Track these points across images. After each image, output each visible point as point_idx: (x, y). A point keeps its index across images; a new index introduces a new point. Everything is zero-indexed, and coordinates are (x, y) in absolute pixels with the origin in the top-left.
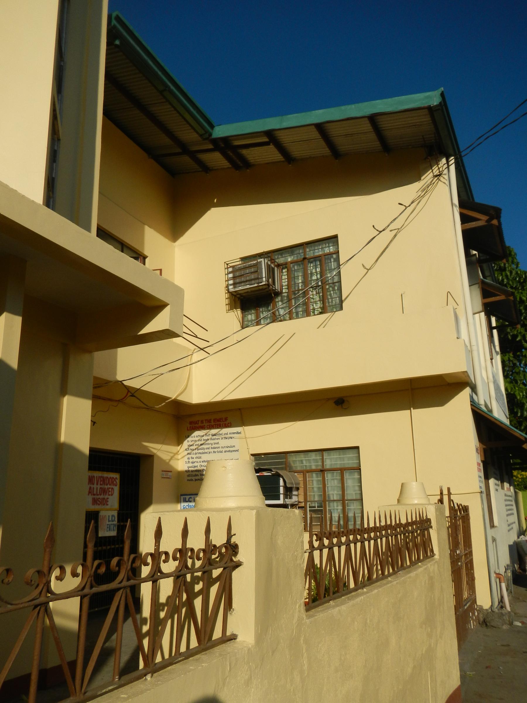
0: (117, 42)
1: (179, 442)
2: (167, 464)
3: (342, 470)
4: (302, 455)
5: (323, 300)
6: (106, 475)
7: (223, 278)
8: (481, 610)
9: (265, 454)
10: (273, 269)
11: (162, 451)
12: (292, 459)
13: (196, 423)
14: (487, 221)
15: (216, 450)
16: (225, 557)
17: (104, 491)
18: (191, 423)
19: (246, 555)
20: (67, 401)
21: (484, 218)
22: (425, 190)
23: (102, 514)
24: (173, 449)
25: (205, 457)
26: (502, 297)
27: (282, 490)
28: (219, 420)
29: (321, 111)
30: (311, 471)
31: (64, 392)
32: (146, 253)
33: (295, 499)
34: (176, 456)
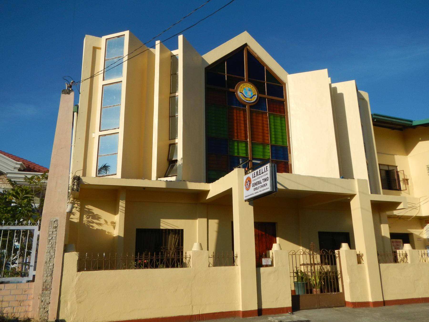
0: (375, 120)
1: (423, 227)
2: (419, 236)
11: (416, 232)
13: (428, 221)
16: (406, 255)
17: (398, 245)
18: (426, 221)
19: (408, 254)
20: (382, 226)
24: (421, 230)
31: (381, 223)
32: (397, 165)
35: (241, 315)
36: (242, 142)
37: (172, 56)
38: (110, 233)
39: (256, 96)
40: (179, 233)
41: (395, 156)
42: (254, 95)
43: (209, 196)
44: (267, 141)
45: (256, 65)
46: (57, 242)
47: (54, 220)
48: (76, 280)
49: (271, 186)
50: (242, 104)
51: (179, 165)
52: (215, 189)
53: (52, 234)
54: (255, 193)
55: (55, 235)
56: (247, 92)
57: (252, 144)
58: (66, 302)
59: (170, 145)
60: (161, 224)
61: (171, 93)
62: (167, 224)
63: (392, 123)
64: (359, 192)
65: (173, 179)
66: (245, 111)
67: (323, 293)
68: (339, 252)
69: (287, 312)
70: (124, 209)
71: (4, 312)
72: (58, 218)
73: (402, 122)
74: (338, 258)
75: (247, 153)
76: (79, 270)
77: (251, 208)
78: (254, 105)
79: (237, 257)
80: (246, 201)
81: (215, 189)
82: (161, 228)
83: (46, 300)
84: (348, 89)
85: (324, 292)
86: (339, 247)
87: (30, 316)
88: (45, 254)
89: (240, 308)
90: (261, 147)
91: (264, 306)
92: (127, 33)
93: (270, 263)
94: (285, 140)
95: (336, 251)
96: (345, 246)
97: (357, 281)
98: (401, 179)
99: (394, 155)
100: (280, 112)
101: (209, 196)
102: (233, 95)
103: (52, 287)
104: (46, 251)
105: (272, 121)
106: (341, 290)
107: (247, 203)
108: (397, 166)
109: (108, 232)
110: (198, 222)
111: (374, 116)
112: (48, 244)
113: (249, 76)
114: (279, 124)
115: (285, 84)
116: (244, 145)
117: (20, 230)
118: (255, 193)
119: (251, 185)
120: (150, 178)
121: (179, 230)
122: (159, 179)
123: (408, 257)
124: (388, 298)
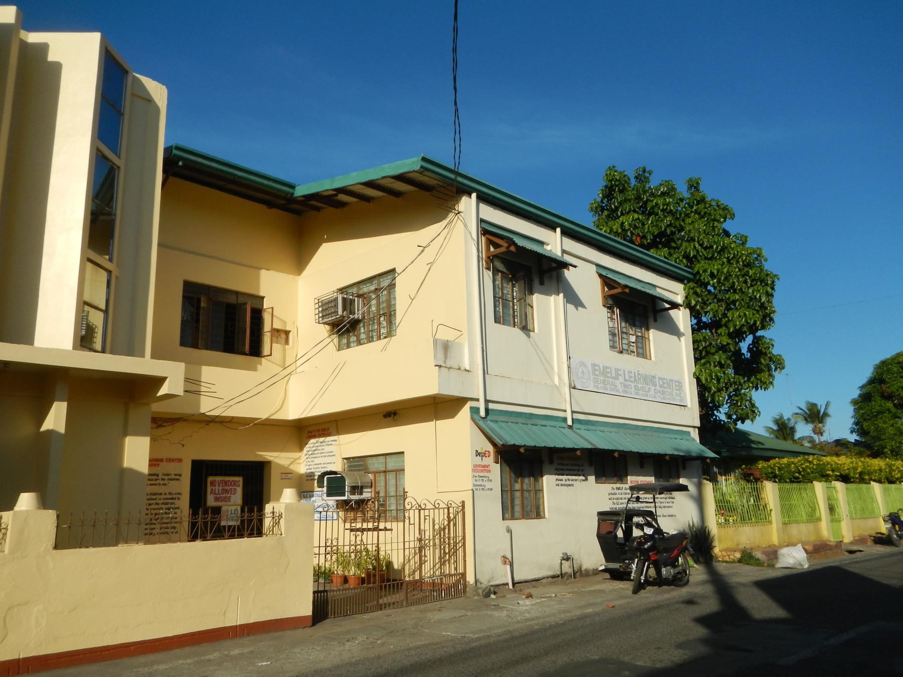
1: (301, 449)
4: (375, 458)
6: (227, 478)
9: (353, 458)
10: (352, 301)
11: (279, 458)
14: (508, 247)
17: (227, 491)
18: (309, 432)
23: (224, 509)
25: (317, 461)
26: (619, 290)
28: (324, 430)
29: (354, 174)
31: (126, 433)
32: (262, 294)
34: (298, 461)
41: (263, 272)
98: (267, 327)
99: (261, 269)
108: (263, 298)
111: (174, 152)
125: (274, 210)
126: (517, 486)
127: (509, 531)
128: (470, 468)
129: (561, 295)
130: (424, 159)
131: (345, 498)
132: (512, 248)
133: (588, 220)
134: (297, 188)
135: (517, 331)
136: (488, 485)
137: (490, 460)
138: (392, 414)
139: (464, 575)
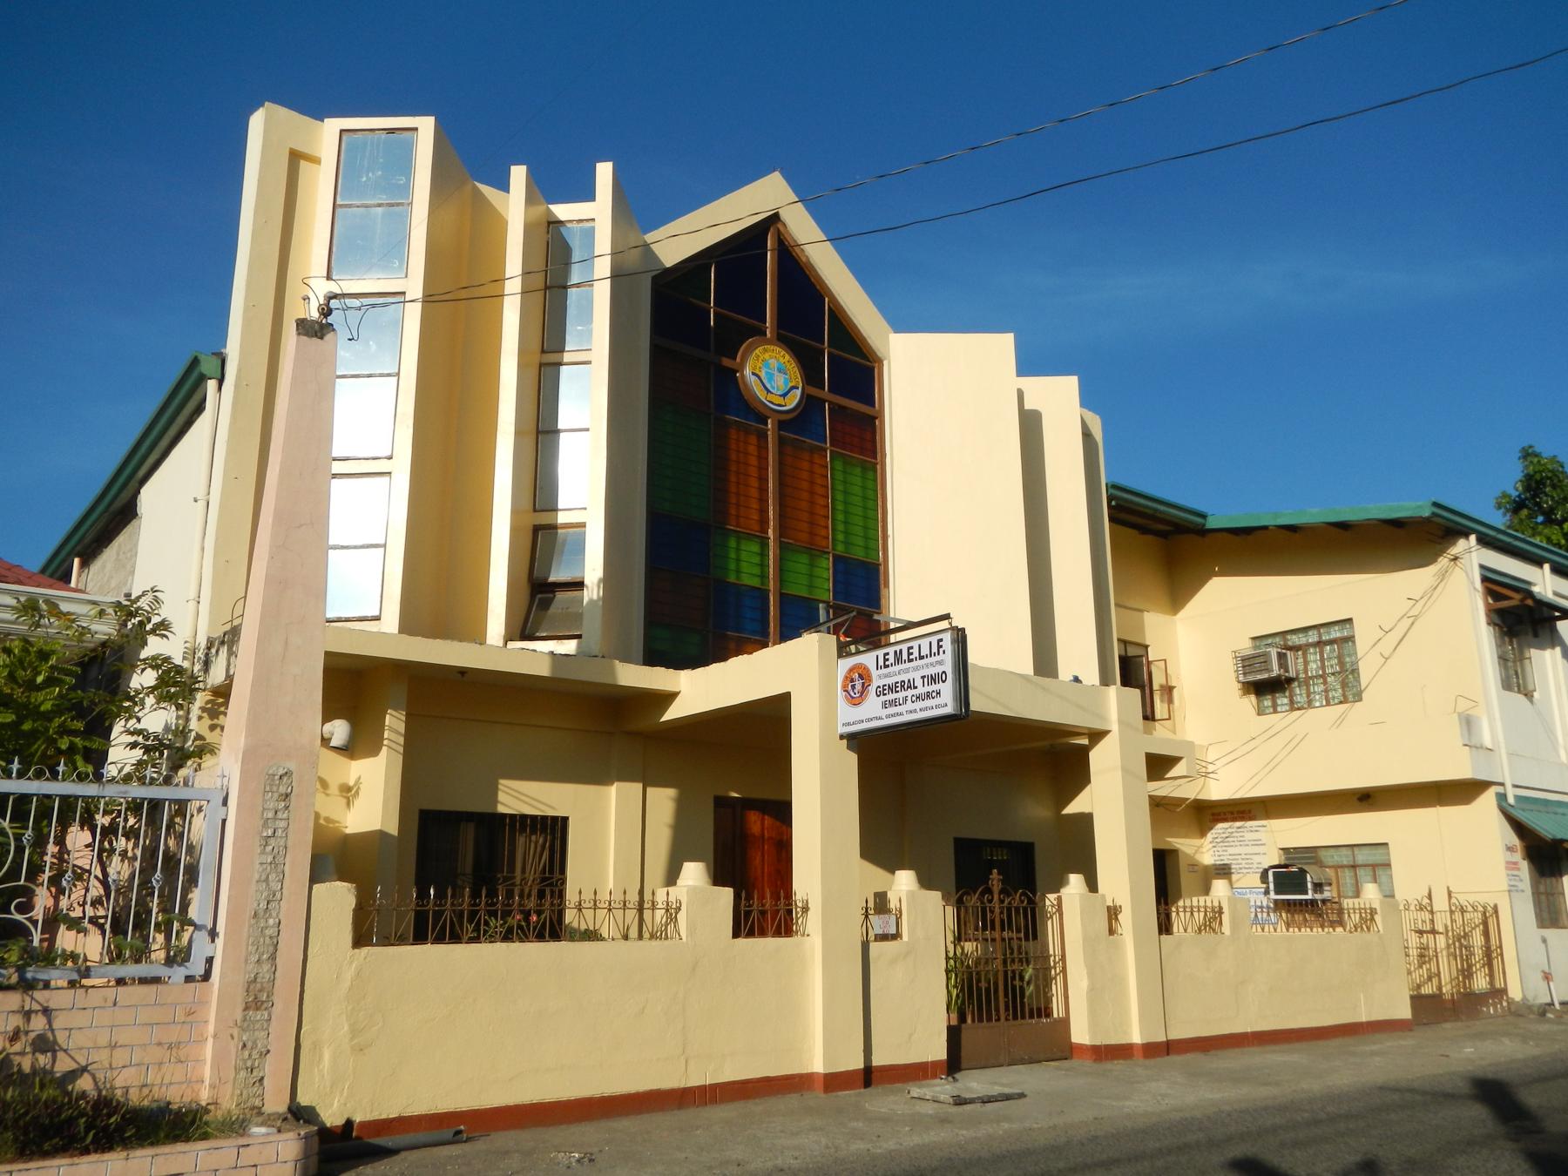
1: (1203, 833)
2: (1193, 858)
3: (1374, 866)
5: (1344, 685)
7: (1232, 668)
8: (1510, 1002)
12: (1322, 853)
14: (1522, 600)
15: (1242, 843)
19: (1226, 910)
21: (1517, 596)
22: (1443, 576)
24: (1197, 842)
25: (1231, 850)
27: (1309, 885)
30: (1342, 867)
33: (1327, 895)
35: (819, 1084)
36: (750, 537)
37: (549, 223)
38: (334, 822)
39: (798, 392)
40: (554, 830)
42: (793, 388)
43: (673, 713)
44: (824, 543)
45: (802, 288)
46: (289, 844)
47: (281, 772)
48: (349, 974)
49: (955, 699)
50: (756, 414)
51: (591, 601)
52: (700, 691)
53: (275, 819)
54: (888, 716)
55: (283, 824)
56: (770, 374)
57: (783, 547)
58: (316, 1046)
59: (537, 529)
60: (501, 797)
61: (543, 351)
62: (519, 797)
63: (1154, 517)
64: (1120, 722)
65: (569, 647)
66: (763, 436)
67: (1020, 1021)
68: (1059, 899)
69: (935, 1076)
70: (401, 740)
71: (118, 1083)
72: (291, 765)
73: (1182, 514)
74: (1056, 918)
75: (764, 576)
76: (360, 940)
77: (852, 759)
78: (791, 421)
79: (806, 909)
80: (842, 737)
81: (700, 691)
82: (501, 809)
83: (255, 1043)
84: (1059, 399)
85: (998, 1020)
86: (1058, 884)
87: (204, 1097)
88: (253, 887)
89: (818, 1066)
90: (804, 559)
91: (877, 1061)
92: (425, 126)
93: (893, 931)
94: (871, 544)
95: (1051, 898)
96: (1076, 881)
97: (1105, 987)
98: (1156, 687)
100: (862, 451)
101: (673, 713)
102: (729, 379)
103: (275, 999)
104: (257, 876)
105: (839, 476)
106: (1057, 1011)
107: (845, 741)
109: (327, 819)
110: (613, 790)
111: (1112, 491)
112: (263, 852)
113: (781, 323)
114: (857, 490)
115: (880, 361)
116: (755, 548)
117: (48, 797)
118: (888, 716)
119: (872, 689)
120: (479, 637)
121: (555, 819)
122: (511, 645)
123: (1226, 918)
124: (1175, 1035)
125: (1150, 538)
126: (1542, 888)
127: (1544, 941)
128: (1502, 866)
129: (1558, 650)
130: (1435, 504)
131: (1309, 897)
132: (1530, 602)
133: (1499, 519)
134: (1210, 519)
135: (1521, 697)
136: (1521, 886)
137: (1518, 856)
138: (1366, 799)
139: (1504, 991)
